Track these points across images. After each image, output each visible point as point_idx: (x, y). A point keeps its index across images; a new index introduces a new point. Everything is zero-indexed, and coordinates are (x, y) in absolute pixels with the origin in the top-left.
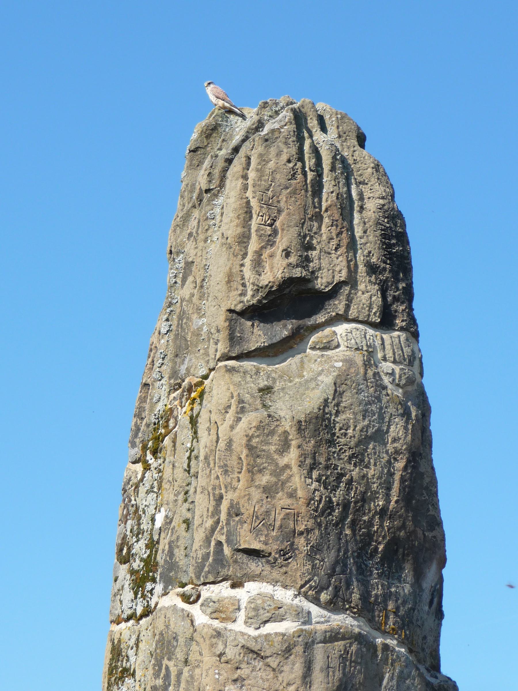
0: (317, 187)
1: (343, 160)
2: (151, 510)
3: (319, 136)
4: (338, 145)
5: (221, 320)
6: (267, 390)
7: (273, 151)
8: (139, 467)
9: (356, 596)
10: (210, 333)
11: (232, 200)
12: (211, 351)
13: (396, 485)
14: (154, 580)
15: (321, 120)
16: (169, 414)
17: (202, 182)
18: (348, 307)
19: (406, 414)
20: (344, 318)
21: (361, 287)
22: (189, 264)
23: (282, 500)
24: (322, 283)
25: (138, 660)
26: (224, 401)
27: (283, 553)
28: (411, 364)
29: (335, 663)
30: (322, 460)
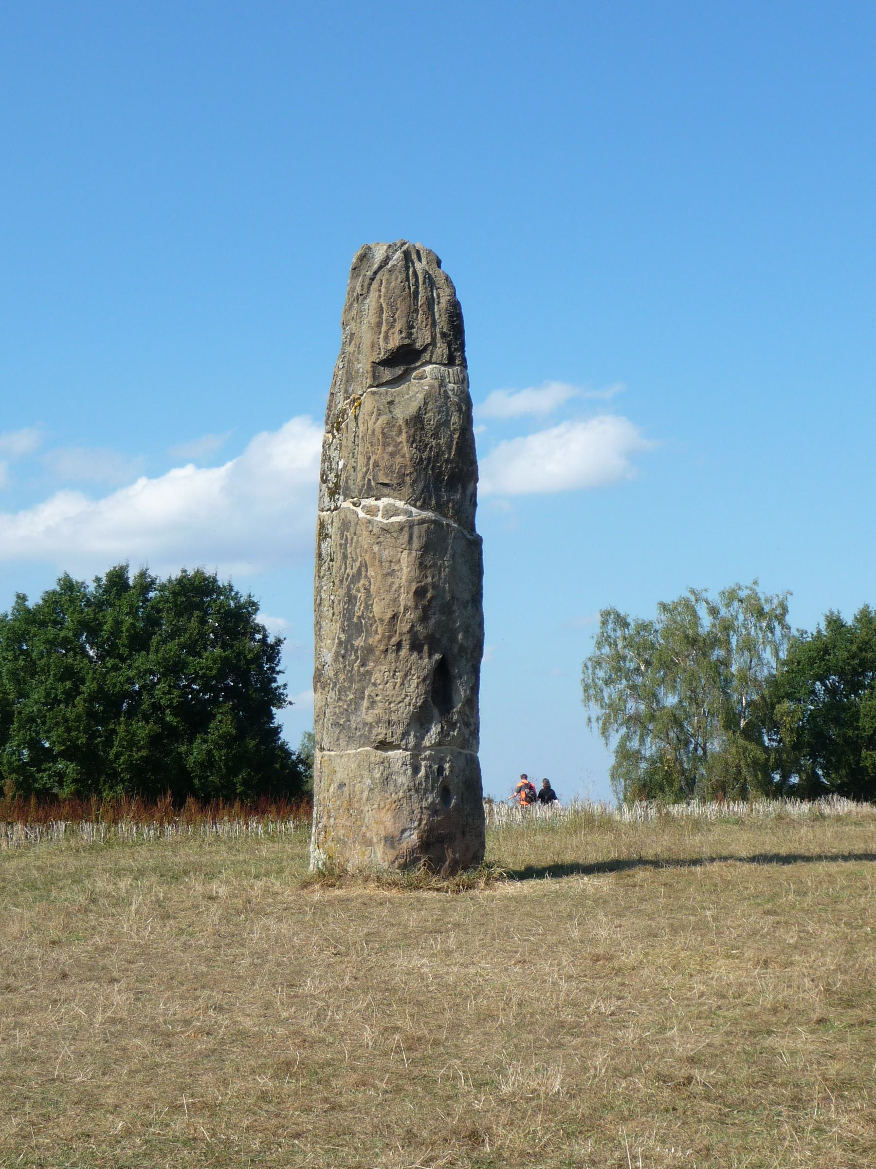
0: (416, 292)
1: (430, 276)
2: (337, 459)
3: (418, 265)
4: (427, 268)
5: (369, 367)
6: (391, 403)
7: (393, 277)
8: (330, 435)
9: (433, 502)
10: (363, 373)
11: (373, 303)
12: (364, 382)
13: (454, 447)
14: (339, 494)
15: (418, 252)
16: (344, 412)
17: (358, 290)
18: (431, 357)
19: (460, 410)
20: (430, 362)
21: (438, 345)
22: (352, 335)
23: (398, 459)
24: (418, 345)
25: (331, 530)
26: (371, 409)
27: (399, 484)
28: (463, 383)
29: (423, 534)
30: (418, 438)
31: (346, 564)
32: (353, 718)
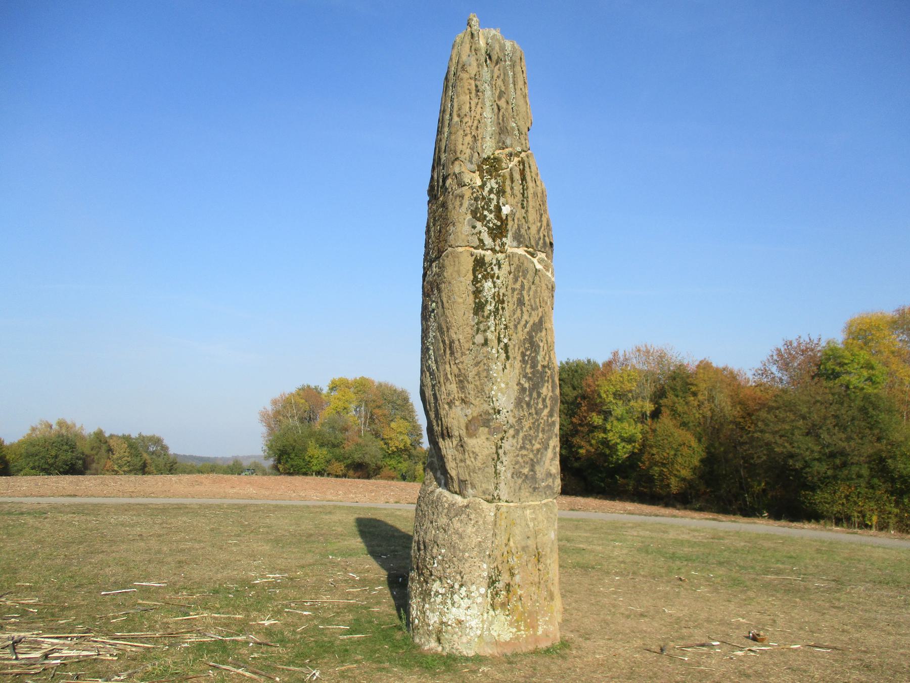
31: (522, 310)
32: (537, 468)
